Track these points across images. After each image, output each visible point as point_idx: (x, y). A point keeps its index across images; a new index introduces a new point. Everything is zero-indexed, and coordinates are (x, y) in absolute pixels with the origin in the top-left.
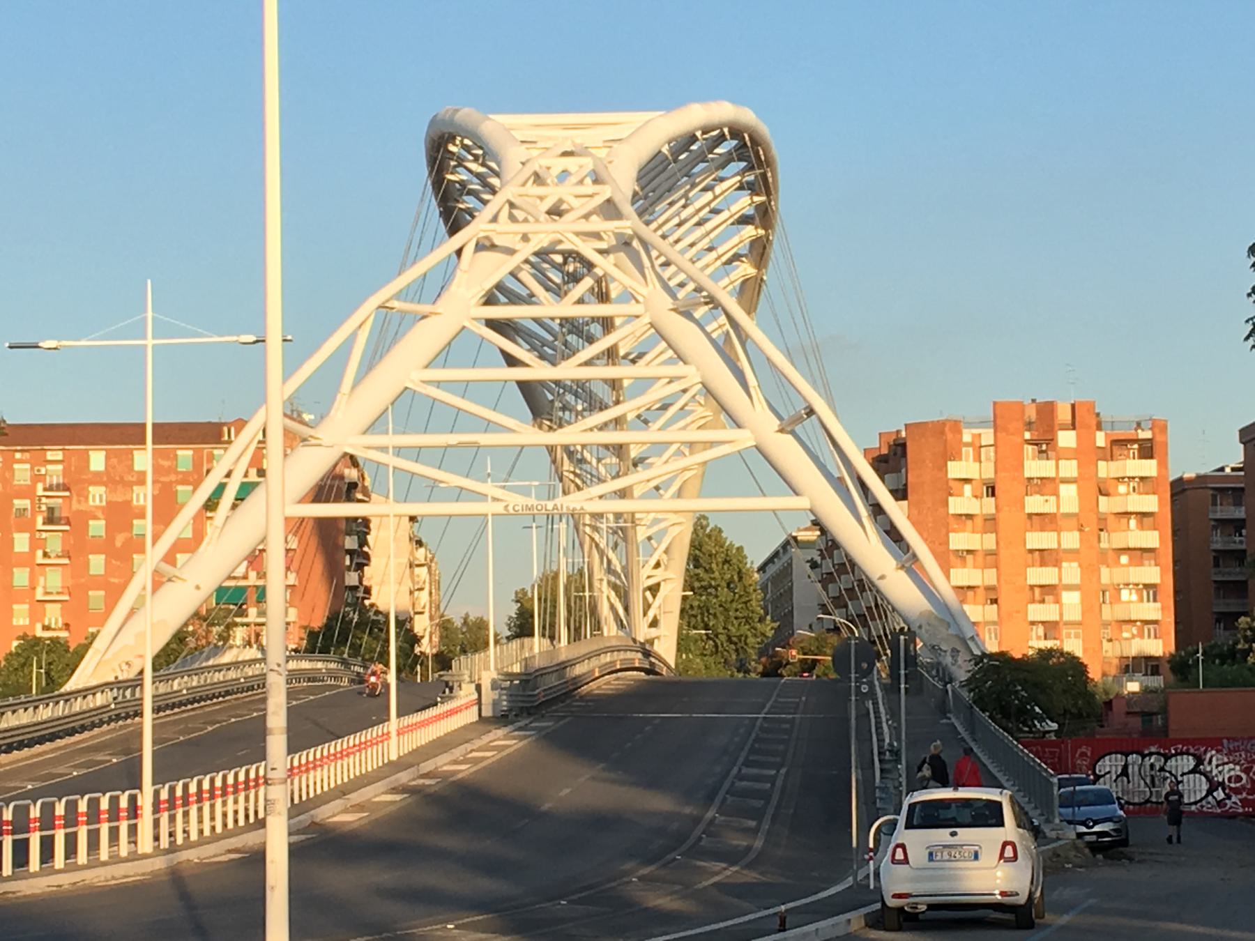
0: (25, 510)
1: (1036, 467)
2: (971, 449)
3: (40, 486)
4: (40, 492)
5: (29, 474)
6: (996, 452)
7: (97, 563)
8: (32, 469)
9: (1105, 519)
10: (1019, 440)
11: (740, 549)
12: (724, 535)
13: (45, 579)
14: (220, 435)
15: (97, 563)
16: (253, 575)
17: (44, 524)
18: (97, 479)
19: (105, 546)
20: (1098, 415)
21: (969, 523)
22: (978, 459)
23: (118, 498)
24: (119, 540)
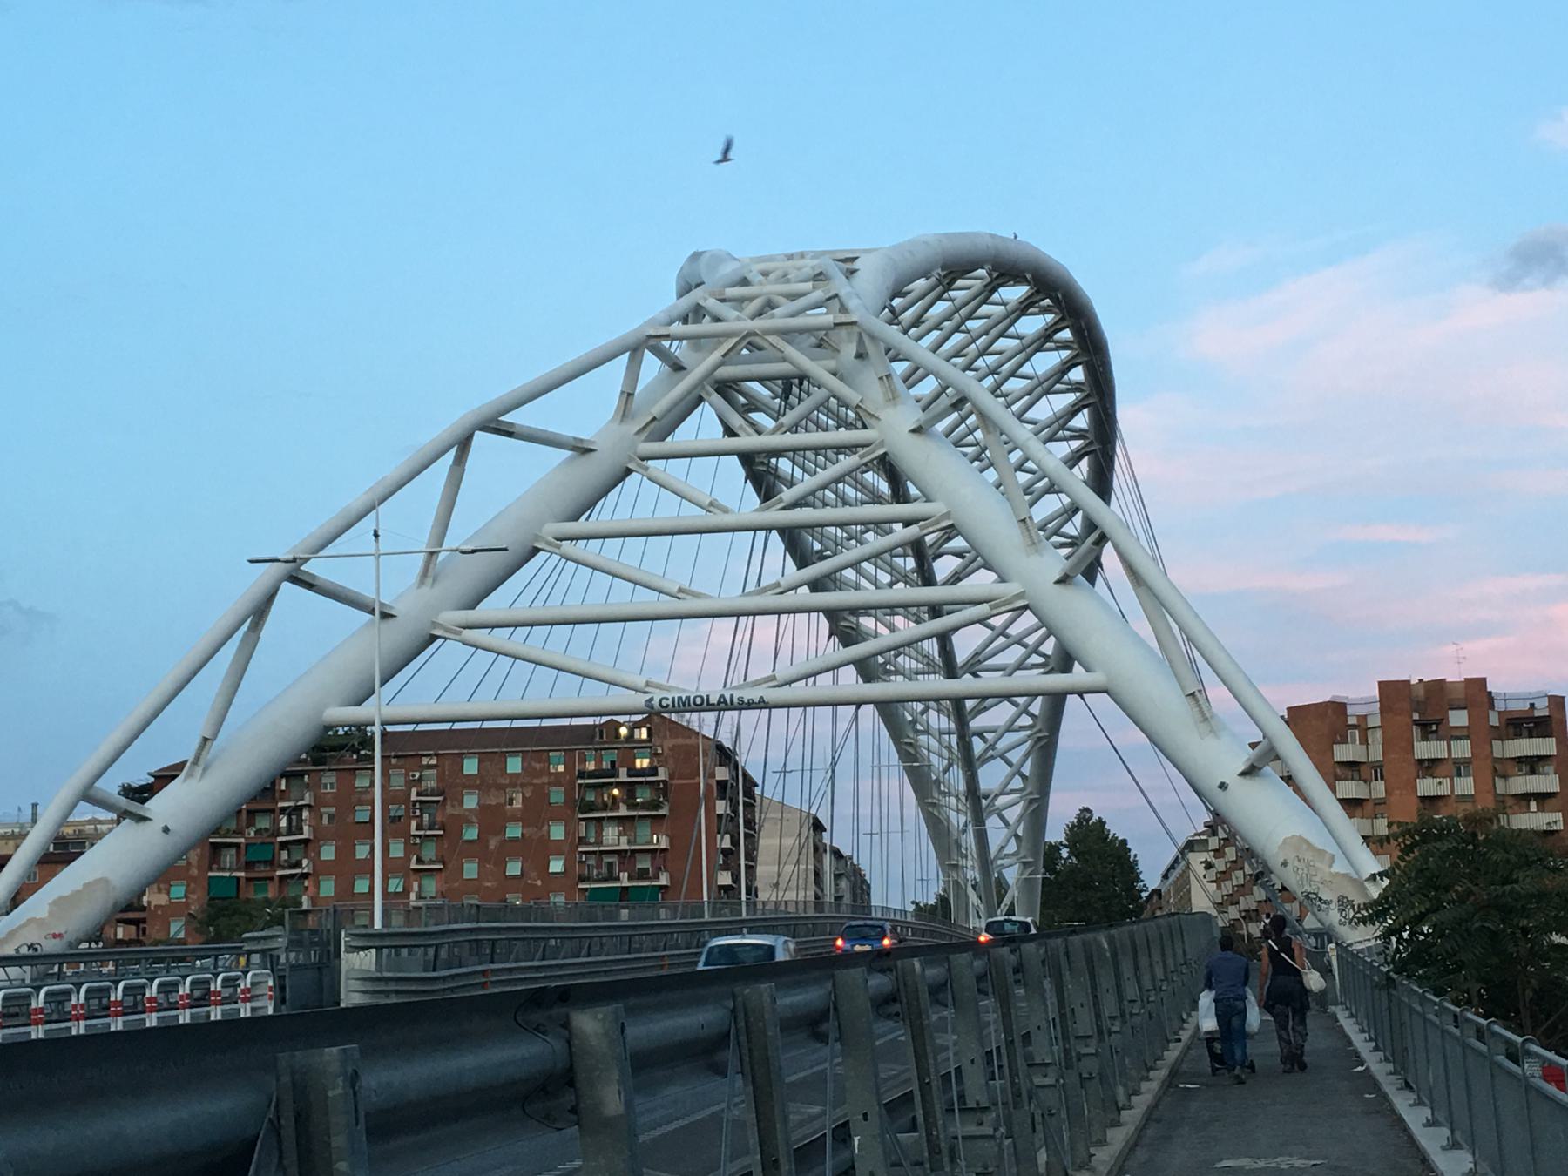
0: (400, 817)
1: (1426, 749)
2: (1357, 732)
3: (414, 791)
4: (414, 797)
5: (403, 779)
6: (1383, 733)
7: (471, 870)
8: (407, 775)
9: (1503, 802)
10: (1409, 721)
11: (1124, 842)
12: (1107, 827)
13: (420, 886)
14: (593, 737)
15: (471, 870)
16: (624, 875)
17: (417, 829)
18: (471, 783)
19: (476, 849)
20: (1490, 693)
21: (1359, 811)
22: (1364, 741)
23: (492, 800)
24: (493, 844)
